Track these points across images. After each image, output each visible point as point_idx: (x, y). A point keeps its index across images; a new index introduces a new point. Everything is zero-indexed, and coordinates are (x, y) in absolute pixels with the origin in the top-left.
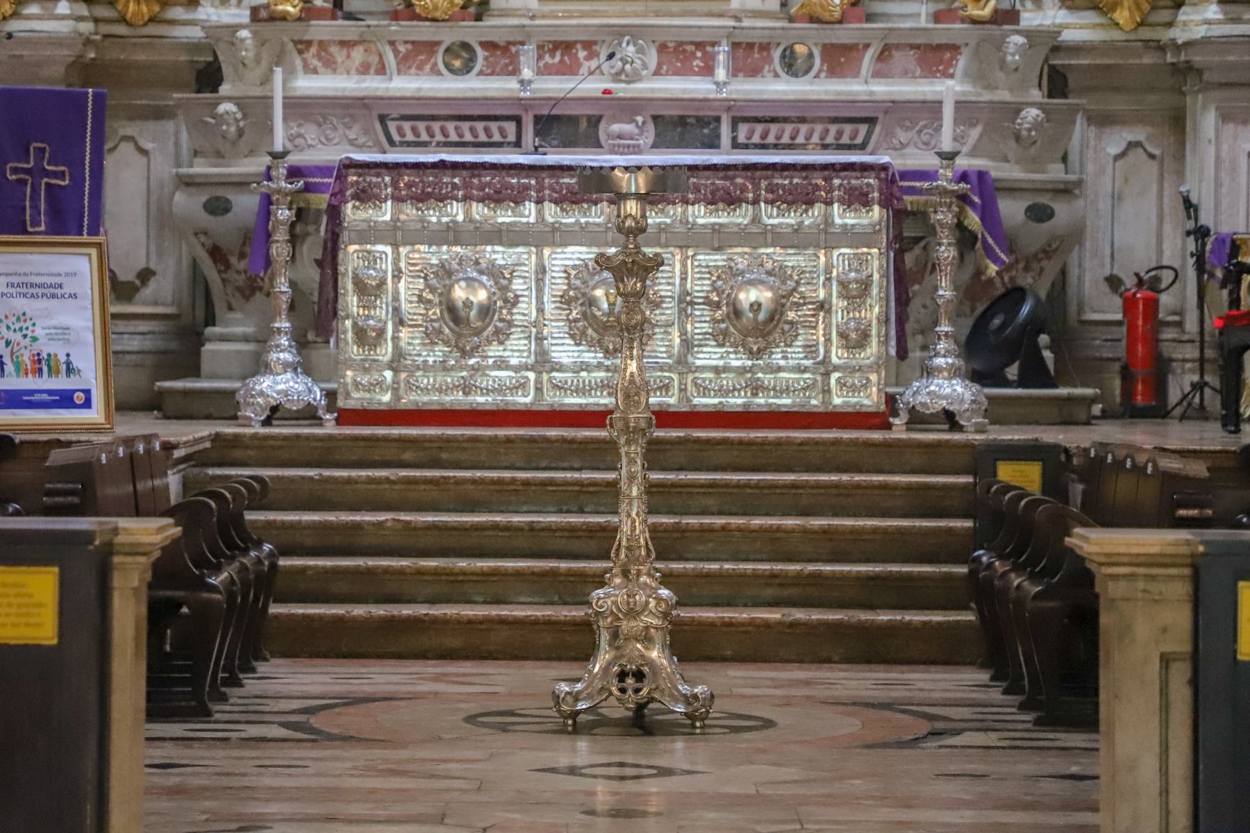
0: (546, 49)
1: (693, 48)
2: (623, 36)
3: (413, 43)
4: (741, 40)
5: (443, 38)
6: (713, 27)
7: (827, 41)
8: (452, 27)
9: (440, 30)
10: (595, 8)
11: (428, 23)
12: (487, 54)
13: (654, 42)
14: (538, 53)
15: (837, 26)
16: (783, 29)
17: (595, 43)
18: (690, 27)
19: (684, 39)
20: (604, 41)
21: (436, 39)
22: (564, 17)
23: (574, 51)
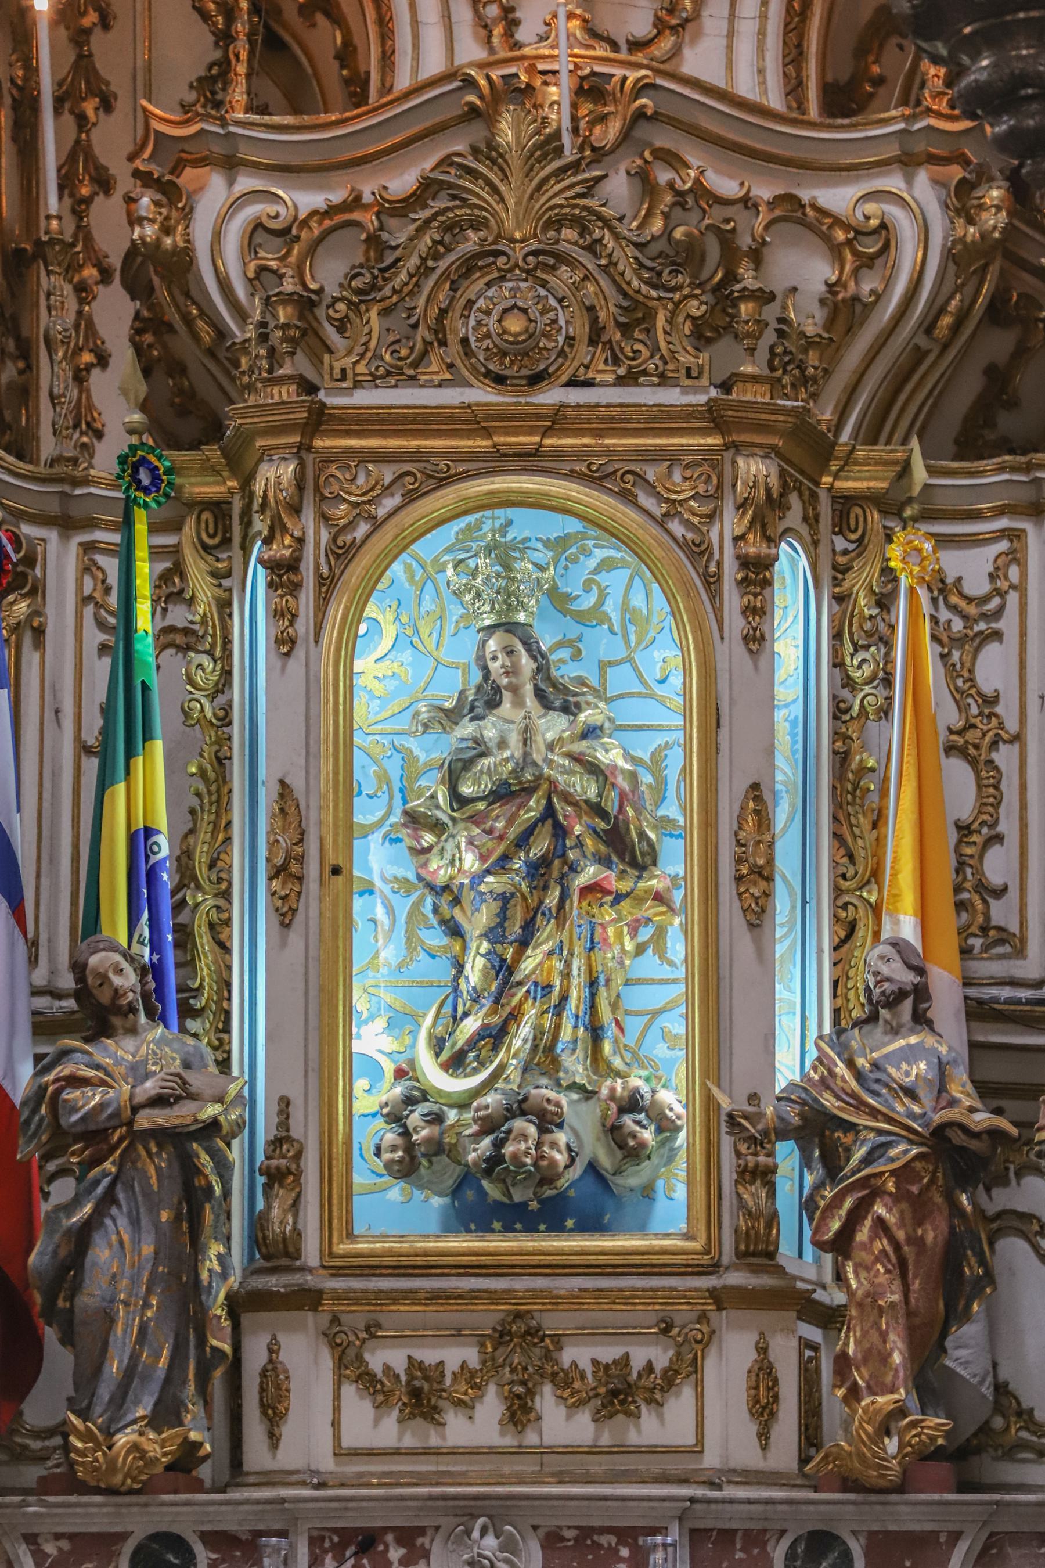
0: (327, 1544)
1: (613, 1540)
2: (474, 1517)
3: (72, 1537)
4: (709, 1524)
5: (130, 1529)
6: (650, 1499)
7: (875, 1527)
8: (146, 1505)
9: (124, 1510)
10: (442, 1468)
11: (98, 1499)
12: (214, 1556)
13: (535, 1528)
14: (312, 1553)
15: (894, 1497)
16: (790, 1502)
17: (421, 1531)
18: (605, 1498)
19: (597, 1523)
20: (437, 1528)
21: (118, 1529)
22: (380, 1485)
23: (381, 1548)
